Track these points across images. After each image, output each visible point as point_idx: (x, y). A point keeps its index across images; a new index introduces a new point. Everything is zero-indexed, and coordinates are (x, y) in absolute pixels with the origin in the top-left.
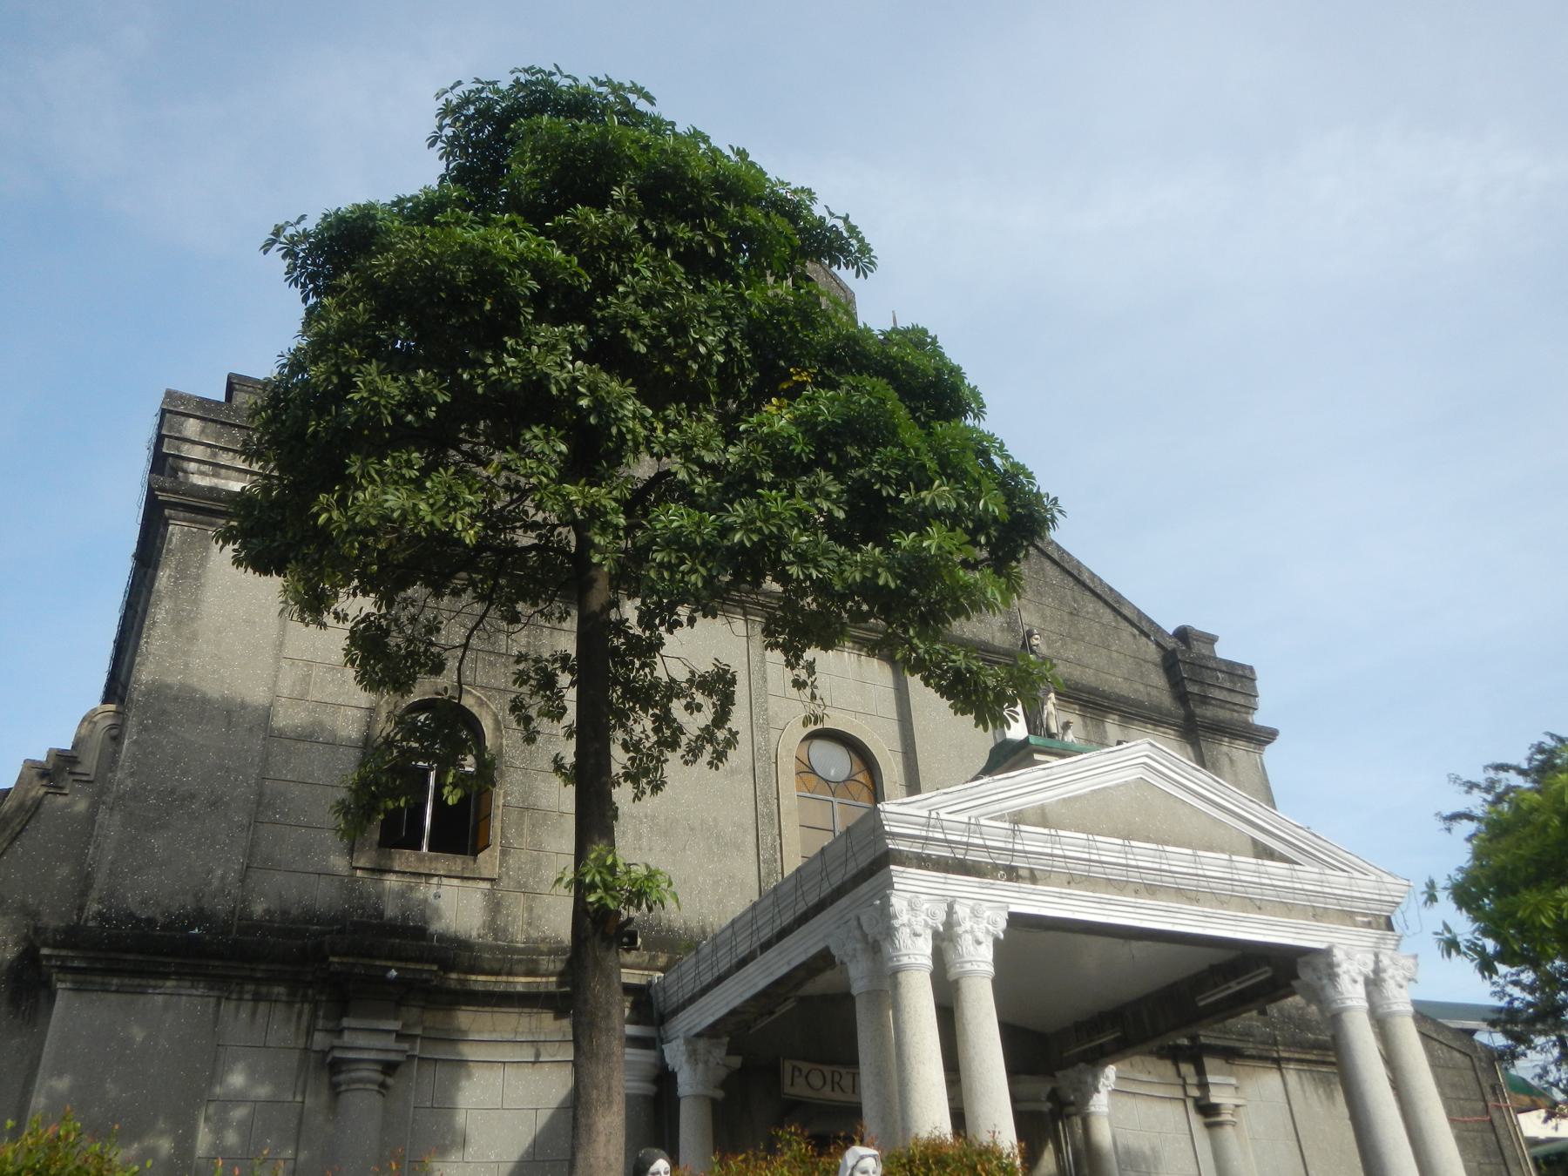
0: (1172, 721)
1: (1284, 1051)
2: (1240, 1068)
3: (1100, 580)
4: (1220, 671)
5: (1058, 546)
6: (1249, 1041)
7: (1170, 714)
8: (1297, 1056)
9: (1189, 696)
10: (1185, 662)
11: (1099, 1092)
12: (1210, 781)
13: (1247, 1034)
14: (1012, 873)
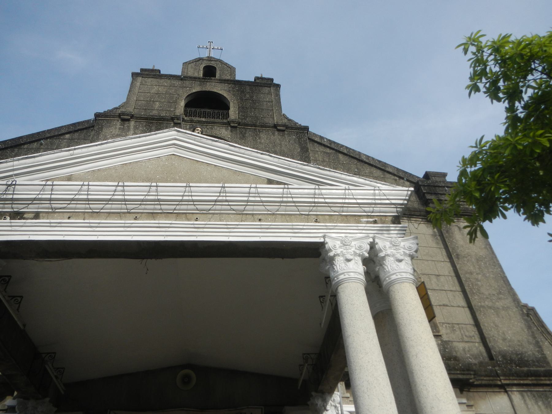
0: (418, 213)
1: (504, 380)
2: (475, 394)
3: (373, 159)
4: (447, 187)
5: (347, 148)
6: (471, 374)
7: (415, 210)
8: (515, 382)
9: (429, 201)
10: (424, 186)
11: (327, 410)
12: (227, 146)
13: (468, 370)
14: (17, 215)
